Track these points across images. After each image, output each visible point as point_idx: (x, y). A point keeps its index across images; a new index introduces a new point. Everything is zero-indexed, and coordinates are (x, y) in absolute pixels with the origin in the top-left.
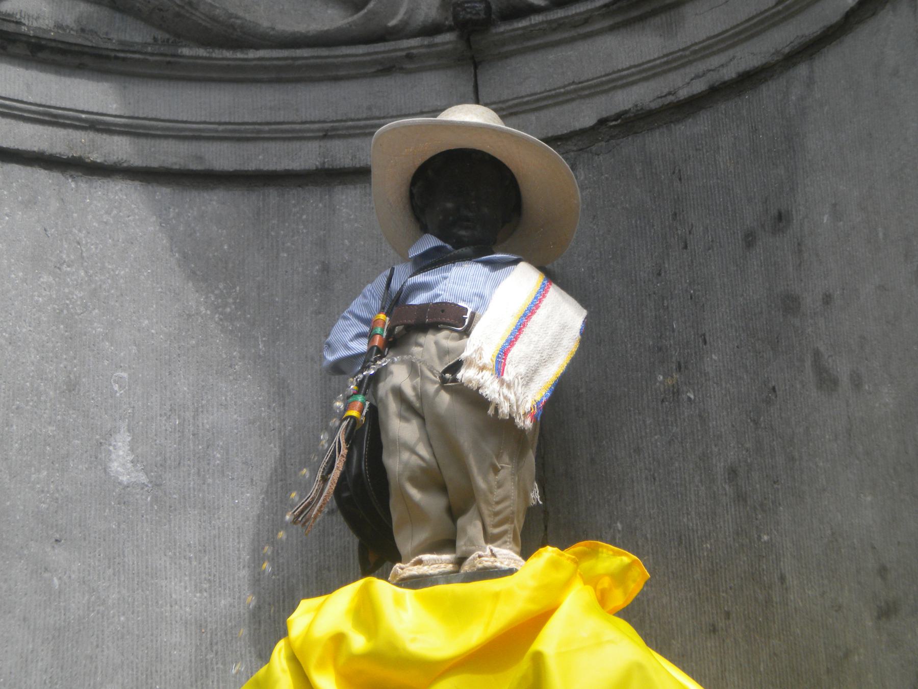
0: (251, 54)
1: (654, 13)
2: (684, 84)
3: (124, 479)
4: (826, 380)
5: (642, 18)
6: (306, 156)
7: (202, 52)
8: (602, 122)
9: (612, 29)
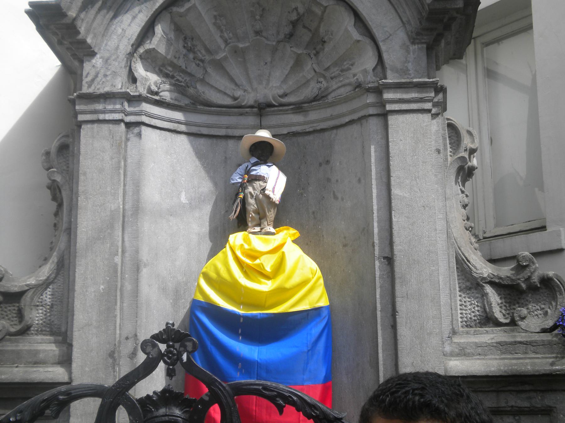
0: (212, 109)
1: (302, 112)
2: (308, 128)
3: (184, 202)
4: (336, 198)
5: (300, 112)
6: (222, 132)
7: (202, 107)
8: (288, 133)
9: (293, 113)
